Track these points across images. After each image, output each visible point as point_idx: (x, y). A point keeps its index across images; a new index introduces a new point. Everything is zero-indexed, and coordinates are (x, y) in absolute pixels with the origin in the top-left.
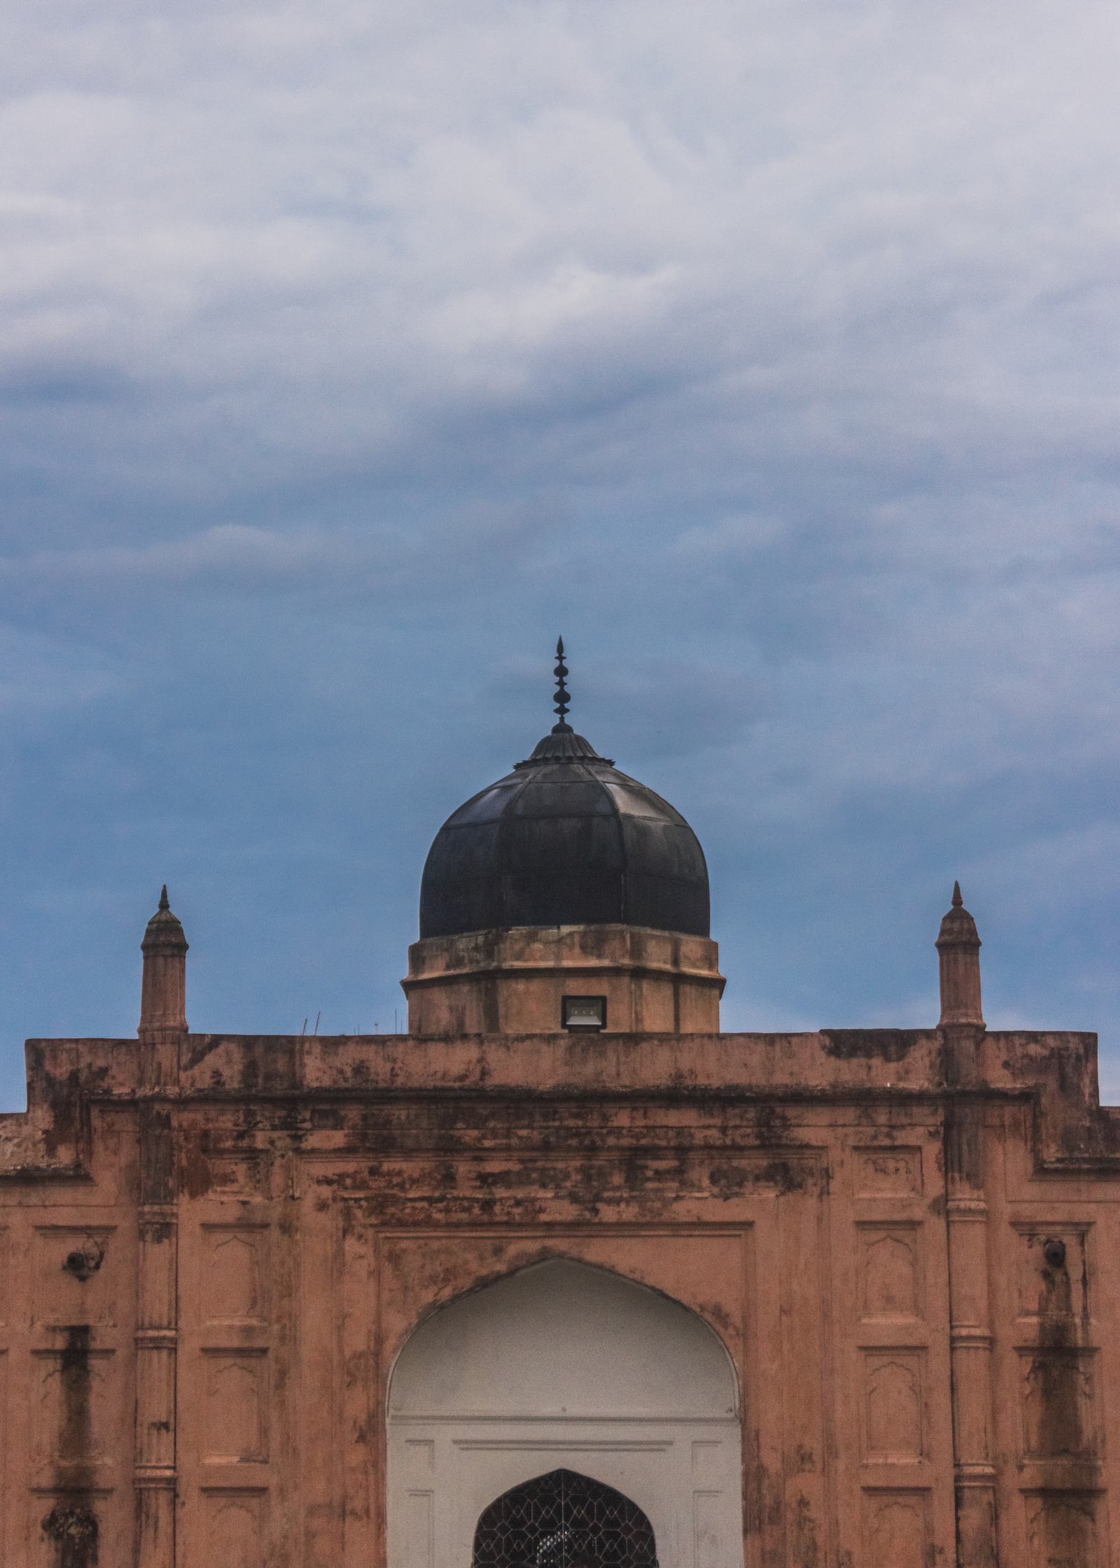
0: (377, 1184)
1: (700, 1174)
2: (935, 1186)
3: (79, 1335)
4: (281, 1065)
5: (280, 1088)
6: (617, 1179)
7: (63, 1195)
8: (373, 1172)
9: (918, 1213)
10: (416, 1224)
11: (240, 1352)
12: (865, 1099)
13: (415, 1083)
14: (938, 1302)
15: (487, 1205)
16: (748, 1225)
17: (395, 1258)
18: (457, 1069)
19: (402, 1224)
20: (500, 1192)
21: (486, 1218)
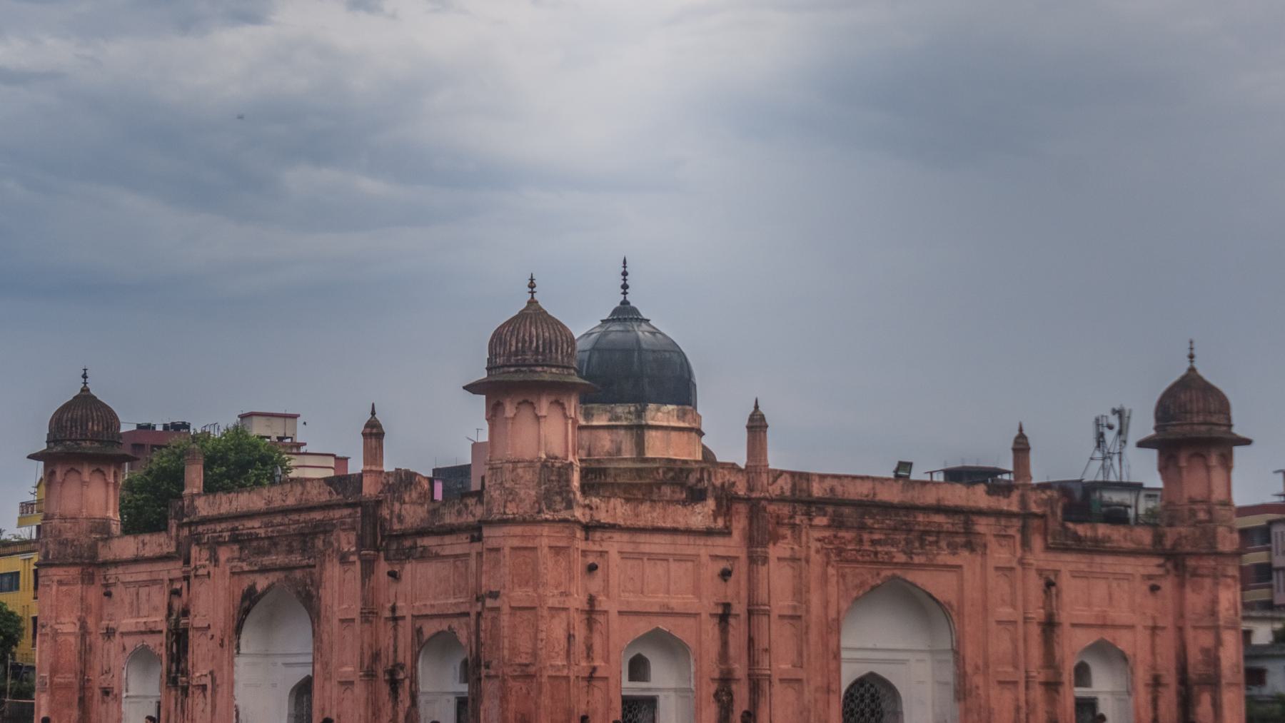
0: (837, 542)
1: (943, 544)
2: (1019, 553)
3: (727, 606)
4: (805, 486)
5: (804, 496)
6: (917, 544)
7: (720, 541)
8: (835, 536)
9: (1014, 564)
10: (852, 561)
11: (792, 617)
12: (998, 514)
13: (851, 497)
14: (1020, 603)
15: (876, 553)
16: (960, 567)
17: (843, 576)
18: (865, 491)
19: (847, 561)
20: (879, 549)
21: (876, 561)
